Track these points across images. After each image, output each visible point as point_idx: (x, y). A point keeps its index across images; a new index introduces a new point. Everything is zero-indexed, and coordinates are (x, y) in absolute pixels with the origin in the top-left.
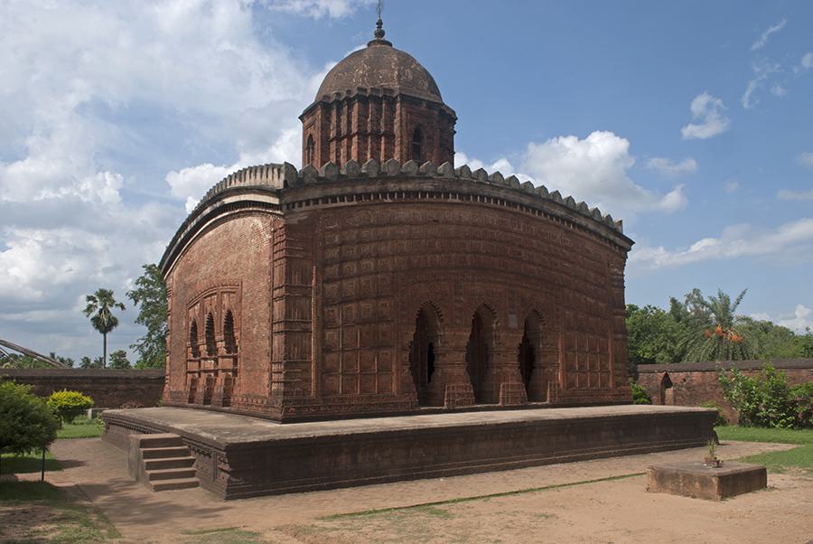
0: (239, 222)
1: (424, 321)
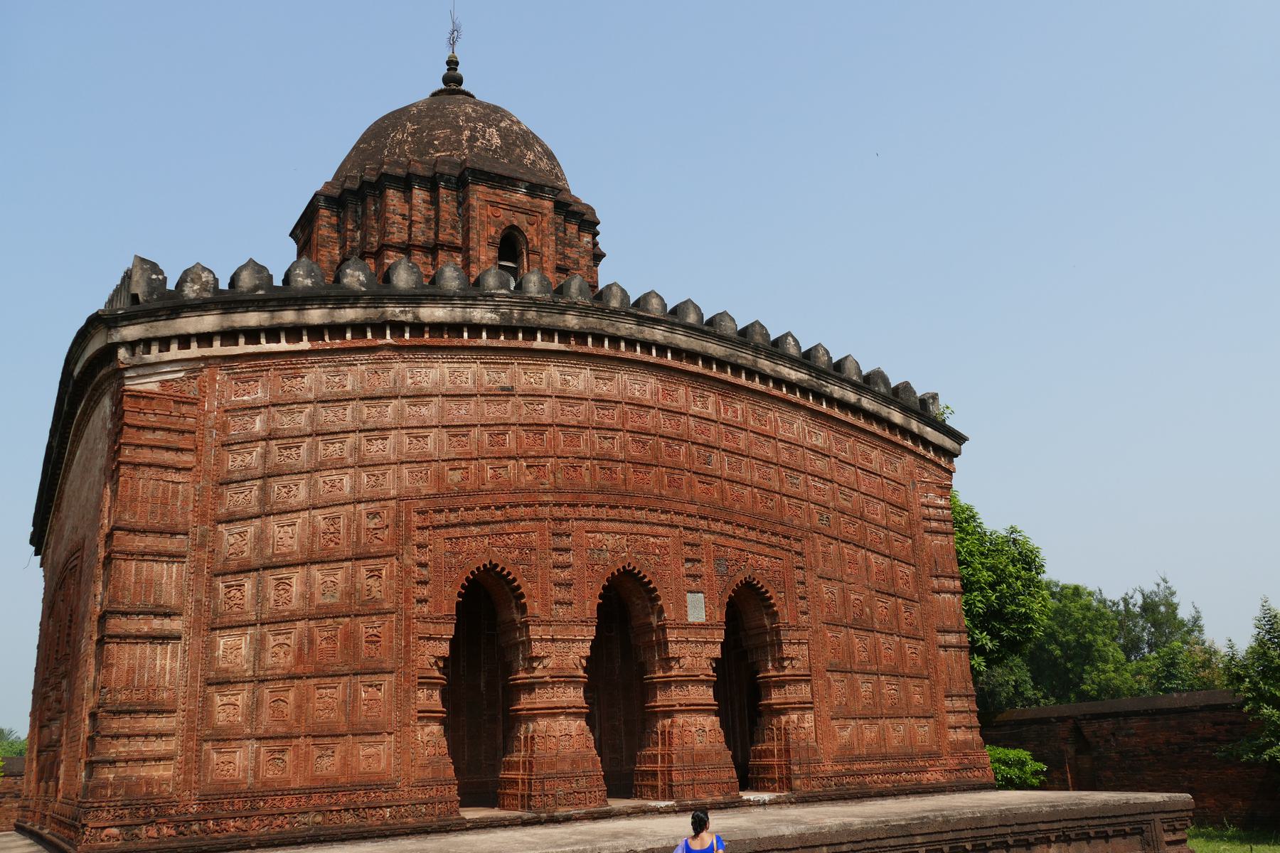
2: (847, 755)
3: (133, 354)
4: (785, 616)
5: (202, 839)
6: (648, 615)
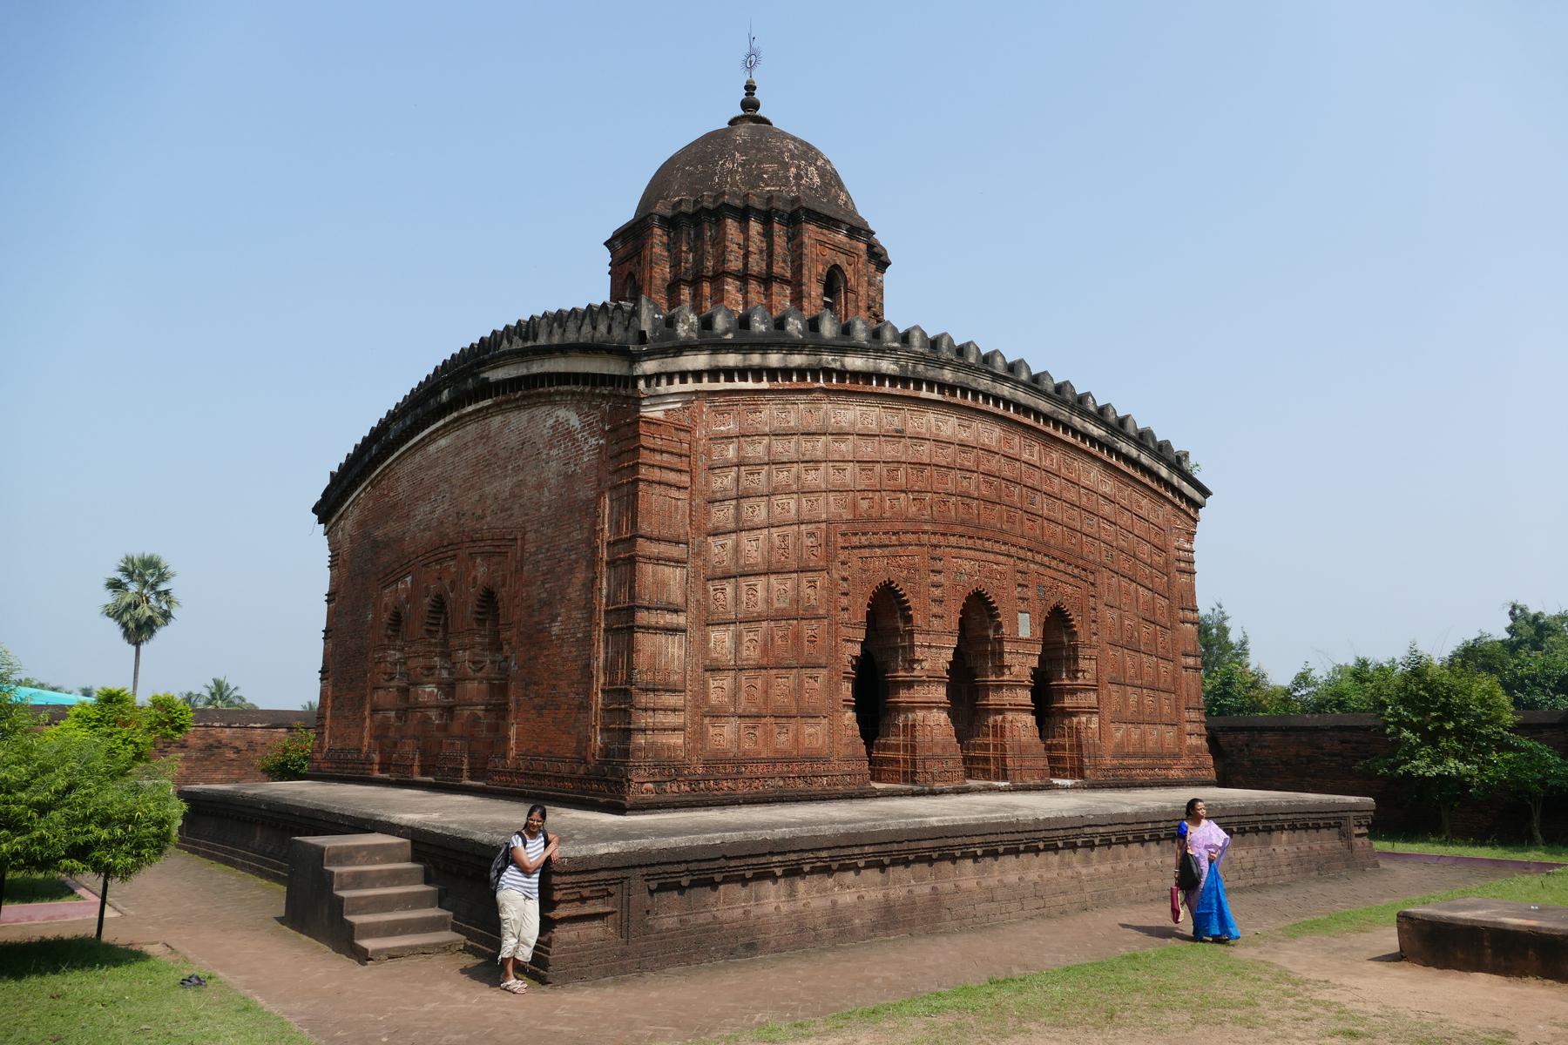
0: (518, 419)
1: (887, 612)
2: (1120, 754)
4: (1082, 636)
6: (987, 628)
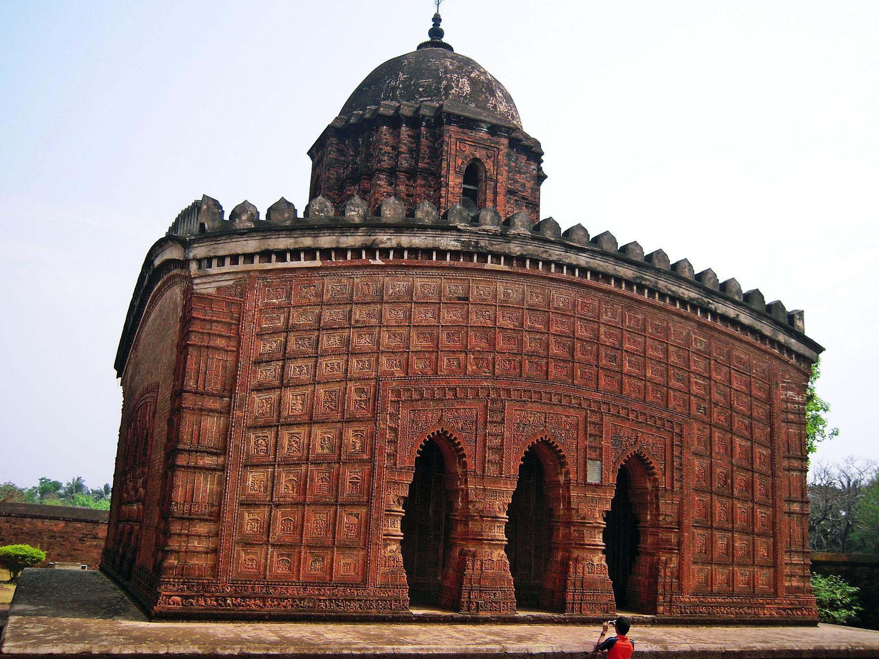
3: (200, 268)
5: (233, 610)
6: (558, 474)
